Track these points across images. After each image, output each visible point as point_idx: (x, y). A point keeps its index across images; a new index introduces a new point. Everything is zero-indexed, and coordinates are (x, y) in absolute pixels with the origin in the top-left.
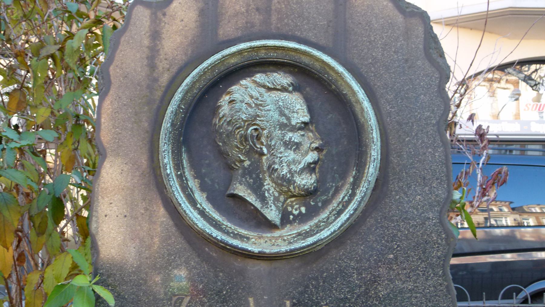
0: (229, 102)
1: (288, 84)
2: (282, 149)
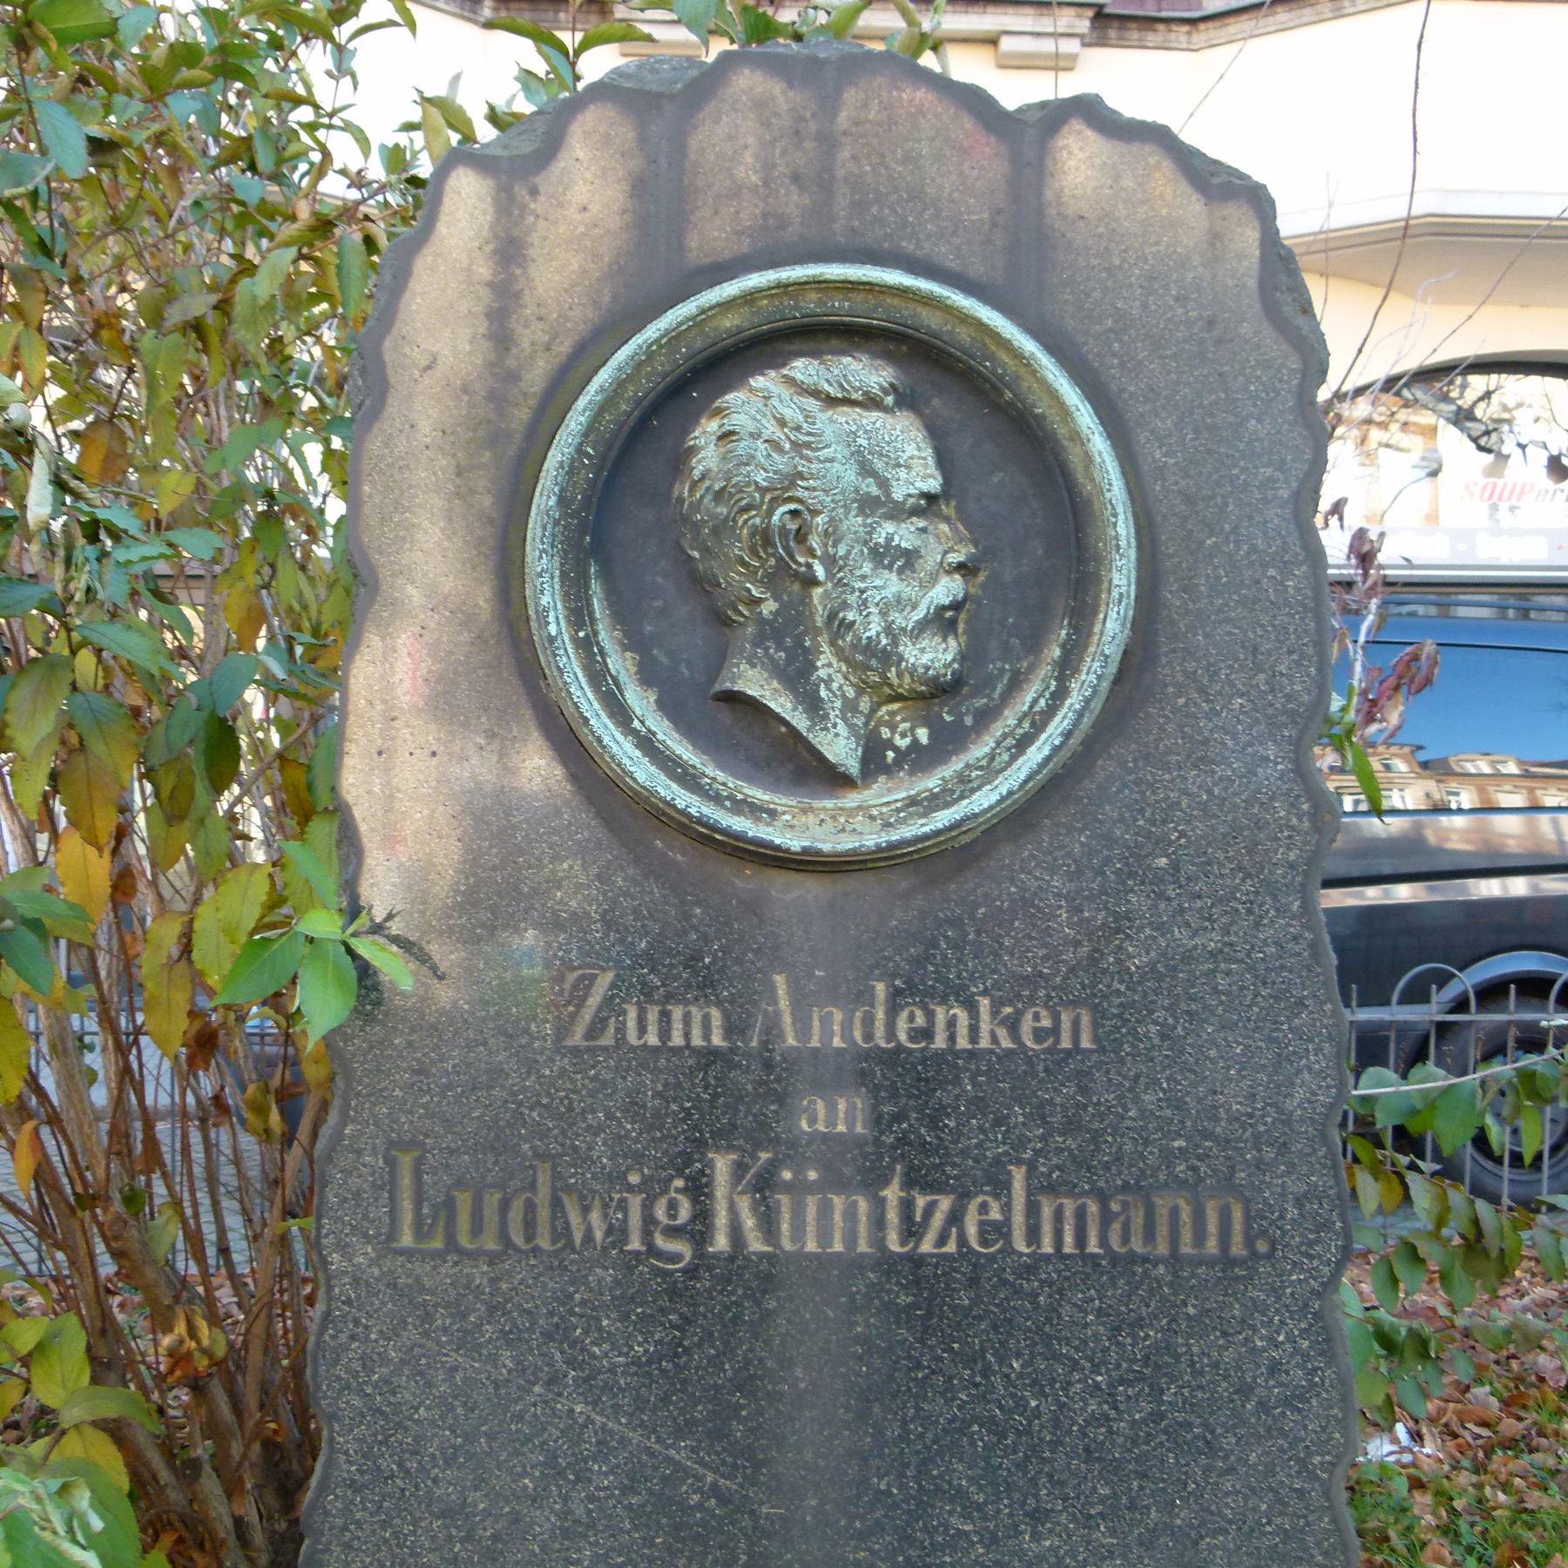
0: (720, 438)
1: (882, 388)
2: (867, 568)
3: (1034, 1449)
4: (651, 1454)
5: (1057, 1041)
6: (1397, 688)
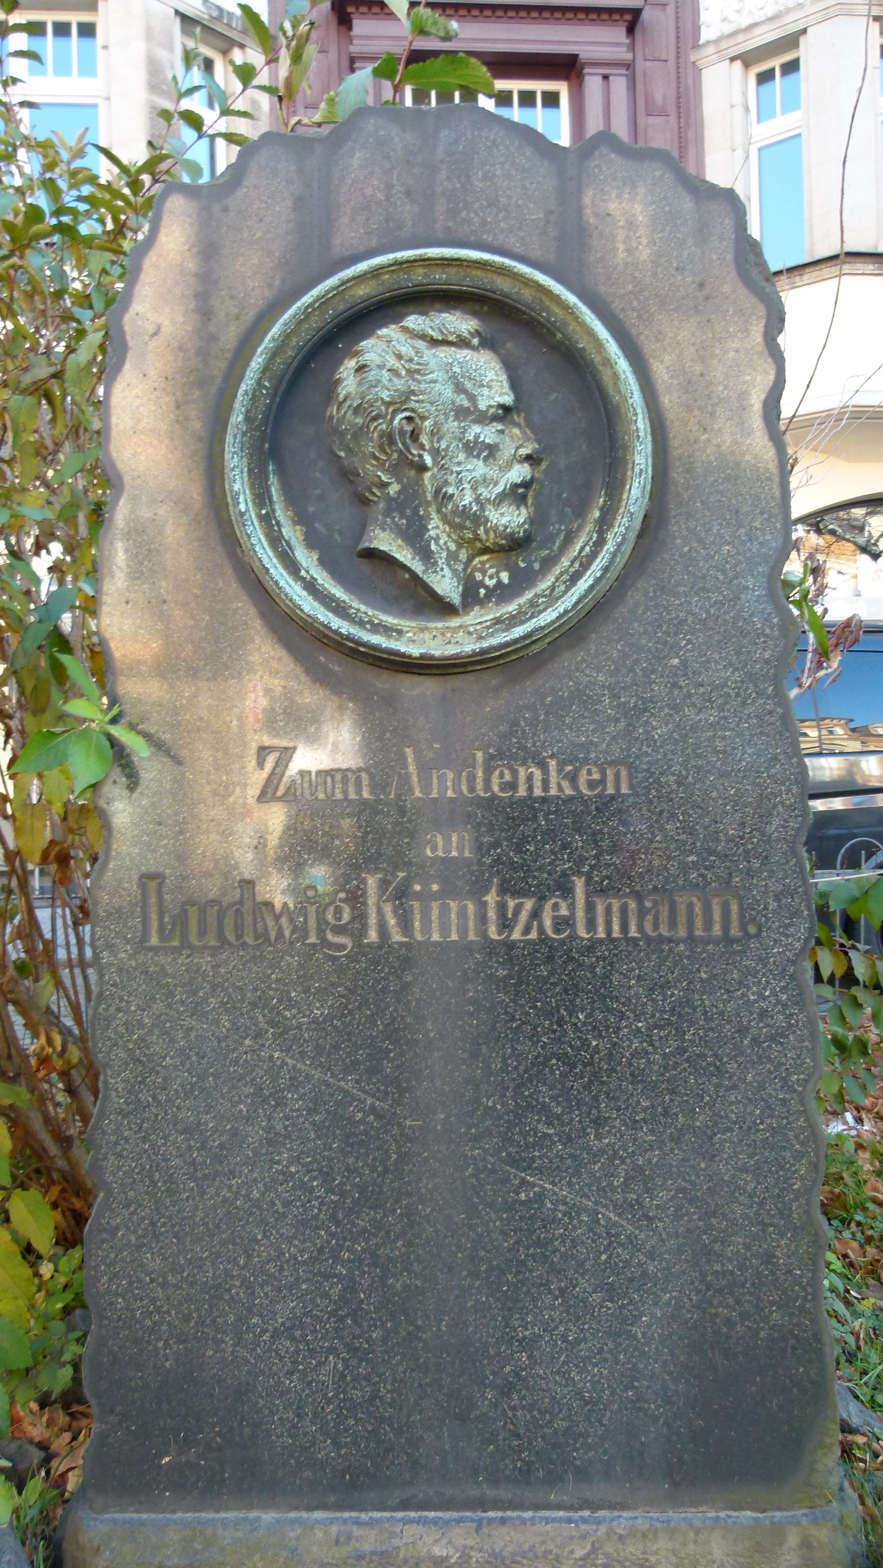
1: (470, 333)
2: (462, 457)
3: (596, 1075)
4: (328, 1086)
5: (605, 789)
6: (837, 645)
